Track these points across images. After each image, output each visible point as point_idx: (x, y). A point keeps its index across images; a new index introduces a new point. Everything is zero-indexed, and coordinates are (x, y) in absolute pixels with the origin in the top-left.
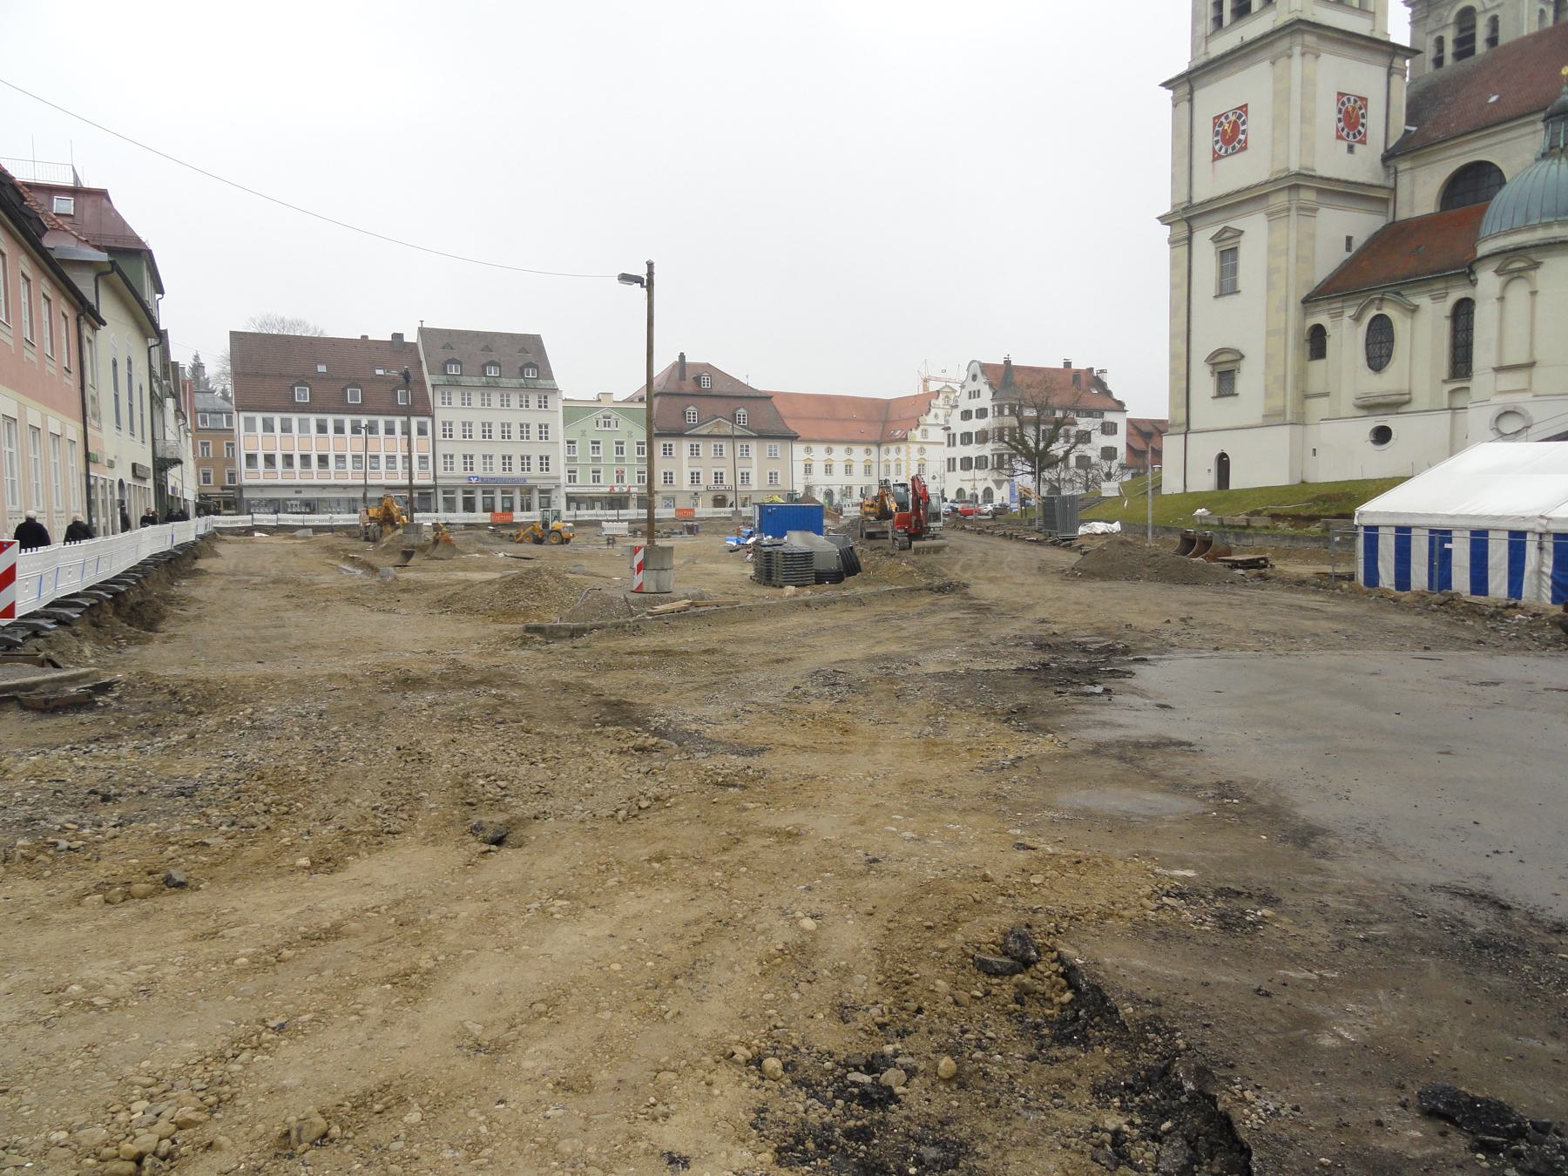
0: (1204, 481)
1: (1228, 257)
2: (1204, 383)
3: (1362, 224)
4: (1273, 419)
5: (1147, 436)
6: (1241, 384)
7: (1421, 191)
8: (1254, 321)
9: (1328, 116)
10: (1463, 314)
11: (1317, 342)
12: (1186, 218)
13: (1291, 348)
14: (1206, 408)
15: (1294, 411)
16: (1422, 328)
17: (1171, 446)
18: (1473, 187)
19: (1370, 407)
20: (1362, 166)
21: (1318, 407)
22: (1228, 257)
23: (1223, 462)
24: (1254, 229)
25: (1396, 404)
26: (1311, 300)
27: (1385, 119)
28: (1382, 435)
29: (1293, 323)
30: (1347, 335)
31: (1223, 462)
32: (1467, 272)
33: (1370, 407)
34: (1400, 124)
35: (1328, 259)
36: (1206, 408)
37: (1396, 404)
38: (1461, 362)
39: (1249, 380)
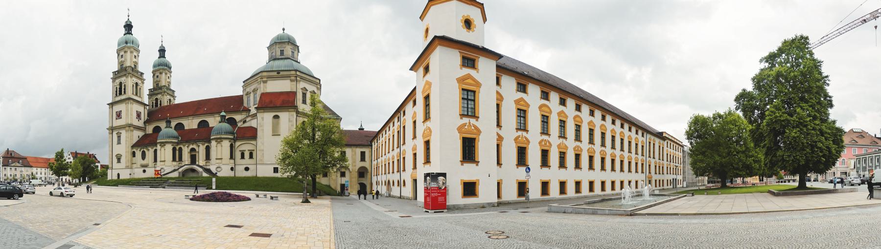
0: (115, 178)
1: (119, 137)
2: (115, 160)
3: (141, 134)
4: (127, 167)
5: (105, 167)
6: (122, 160)
7: (150, 129)
8: (123, 149)
9: (135, 115)
10: (155, 151)
11: (134, 154)
12: (112, 129)
13: (130, 156)
14: (116, 165)
15: (130, 166)
16: (150, 153)
17: (109, 171)
18: (157, 130)
19: (143, 166)
20: (140, 124)
21: (134, 166)
22: (119, 137)
23: (118, 175)
24: (124, 133)
25: (146, 166)
26: (133, 147)
27: (144, 116)
28: (144, 171)
29: (130, 150)
30: (139, 154)
31: (118, 175)
32: (156, 145)
33: (143, 166)
34: (146, 117)
35: (135, 139)
36: (116, 165)
37: (146, 166)
38: (155, 160)
39: (123, 160)
